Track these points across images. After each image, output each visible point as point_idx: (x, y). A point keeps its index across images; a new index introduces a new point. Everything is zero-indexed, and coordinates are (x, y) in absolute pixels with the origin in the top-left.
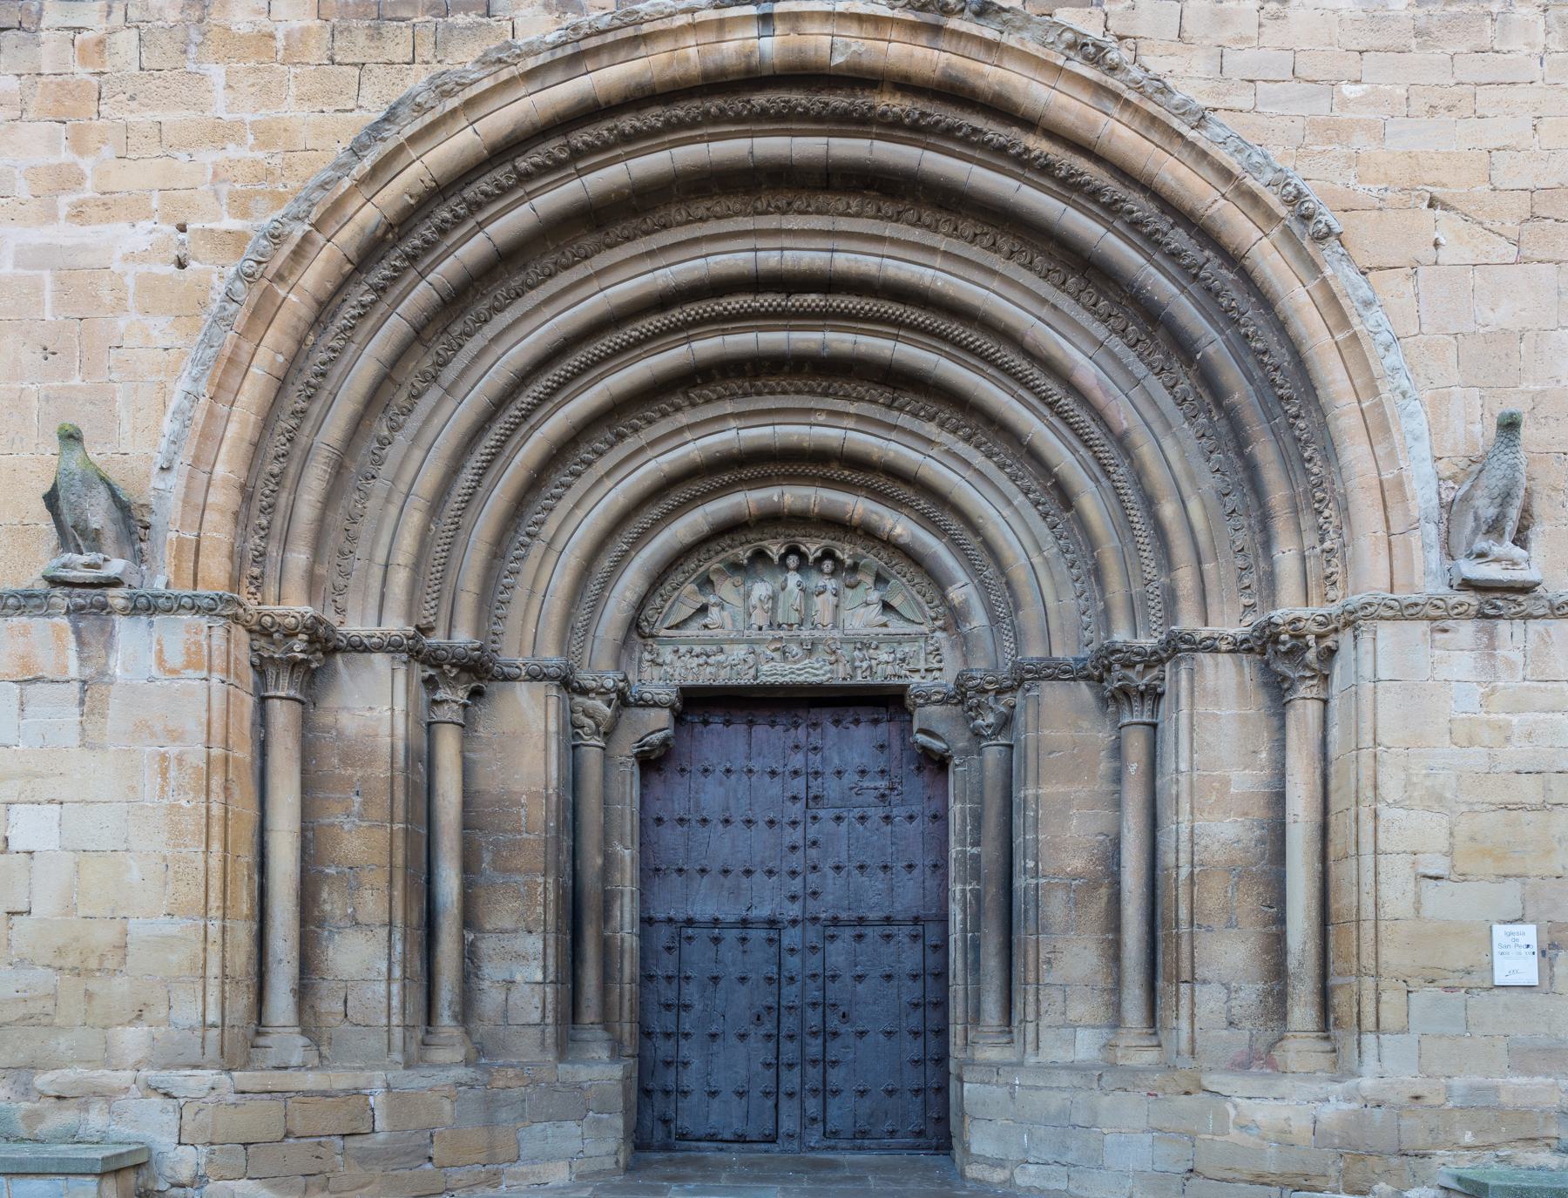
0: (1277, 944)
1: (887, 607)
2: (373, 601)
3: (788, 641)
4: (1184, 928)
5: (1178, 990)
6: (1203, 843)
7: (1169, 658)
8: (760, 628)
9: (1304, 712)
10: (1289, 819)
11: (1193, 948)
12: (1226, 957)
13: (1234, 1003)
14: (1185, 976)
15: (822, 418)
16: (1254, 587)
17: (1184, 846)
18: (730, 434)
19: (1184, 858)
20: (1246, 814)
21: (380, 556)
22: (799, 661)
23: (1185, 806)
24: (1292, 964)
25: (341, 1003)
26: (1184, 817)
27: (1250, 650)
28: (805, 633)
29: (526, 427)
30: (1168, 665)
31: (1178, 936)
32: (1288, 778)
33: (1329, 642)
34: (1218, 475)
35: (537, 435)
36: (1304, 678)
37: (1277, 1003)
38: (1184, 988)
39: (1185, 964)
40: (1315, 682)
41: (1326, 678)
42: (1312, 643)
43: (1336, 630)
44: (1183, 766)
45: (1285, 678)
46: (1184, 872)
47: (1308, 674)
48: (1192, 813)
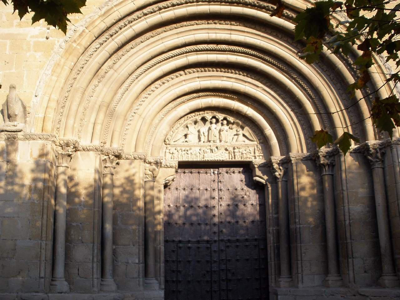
0: (376, 245)
1: (244, 135)
2: (90, 135)
3: (213, 146)
4: (349, 241)
5: (348, 260)
6: (352, 213)
7: (336, 154)
8: (204, 142)
9: (378, 172)
10: (377, 205)
11: (352, 247)
12: (361, 249)
13: (365, 264)
14: (350, 256)
15: (225, 79)
16: (359, 134)
17: (347, 214)
18: (198, 83)
19: (347, 217)
20: (363, 203)
21: (92, 120)
22: (217, 153)
23: (346, 201)
24: (383, 251)
25: (77, 270)
26: (346, 205)
27: (360, 152)
28: (218, 143)
29: (136, 81)
30: (336, 157)
31: (347, 243)
32: (375, 192)
33: (383, 151)
34: (345, 100)
35: (140, 83)
36: (377, 161)
37: (378, 265)
38: (350, 260)
39: (350, 253)
40: (380, 163)
41: (383, 162)
42: (378, 151)
43: (385, 147)
44: (345, 188)
45: (371, 161)
46: (347, 222)
47: (378, 160)
48: (348, 203)
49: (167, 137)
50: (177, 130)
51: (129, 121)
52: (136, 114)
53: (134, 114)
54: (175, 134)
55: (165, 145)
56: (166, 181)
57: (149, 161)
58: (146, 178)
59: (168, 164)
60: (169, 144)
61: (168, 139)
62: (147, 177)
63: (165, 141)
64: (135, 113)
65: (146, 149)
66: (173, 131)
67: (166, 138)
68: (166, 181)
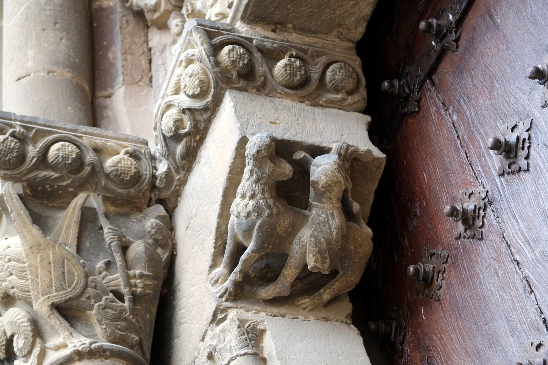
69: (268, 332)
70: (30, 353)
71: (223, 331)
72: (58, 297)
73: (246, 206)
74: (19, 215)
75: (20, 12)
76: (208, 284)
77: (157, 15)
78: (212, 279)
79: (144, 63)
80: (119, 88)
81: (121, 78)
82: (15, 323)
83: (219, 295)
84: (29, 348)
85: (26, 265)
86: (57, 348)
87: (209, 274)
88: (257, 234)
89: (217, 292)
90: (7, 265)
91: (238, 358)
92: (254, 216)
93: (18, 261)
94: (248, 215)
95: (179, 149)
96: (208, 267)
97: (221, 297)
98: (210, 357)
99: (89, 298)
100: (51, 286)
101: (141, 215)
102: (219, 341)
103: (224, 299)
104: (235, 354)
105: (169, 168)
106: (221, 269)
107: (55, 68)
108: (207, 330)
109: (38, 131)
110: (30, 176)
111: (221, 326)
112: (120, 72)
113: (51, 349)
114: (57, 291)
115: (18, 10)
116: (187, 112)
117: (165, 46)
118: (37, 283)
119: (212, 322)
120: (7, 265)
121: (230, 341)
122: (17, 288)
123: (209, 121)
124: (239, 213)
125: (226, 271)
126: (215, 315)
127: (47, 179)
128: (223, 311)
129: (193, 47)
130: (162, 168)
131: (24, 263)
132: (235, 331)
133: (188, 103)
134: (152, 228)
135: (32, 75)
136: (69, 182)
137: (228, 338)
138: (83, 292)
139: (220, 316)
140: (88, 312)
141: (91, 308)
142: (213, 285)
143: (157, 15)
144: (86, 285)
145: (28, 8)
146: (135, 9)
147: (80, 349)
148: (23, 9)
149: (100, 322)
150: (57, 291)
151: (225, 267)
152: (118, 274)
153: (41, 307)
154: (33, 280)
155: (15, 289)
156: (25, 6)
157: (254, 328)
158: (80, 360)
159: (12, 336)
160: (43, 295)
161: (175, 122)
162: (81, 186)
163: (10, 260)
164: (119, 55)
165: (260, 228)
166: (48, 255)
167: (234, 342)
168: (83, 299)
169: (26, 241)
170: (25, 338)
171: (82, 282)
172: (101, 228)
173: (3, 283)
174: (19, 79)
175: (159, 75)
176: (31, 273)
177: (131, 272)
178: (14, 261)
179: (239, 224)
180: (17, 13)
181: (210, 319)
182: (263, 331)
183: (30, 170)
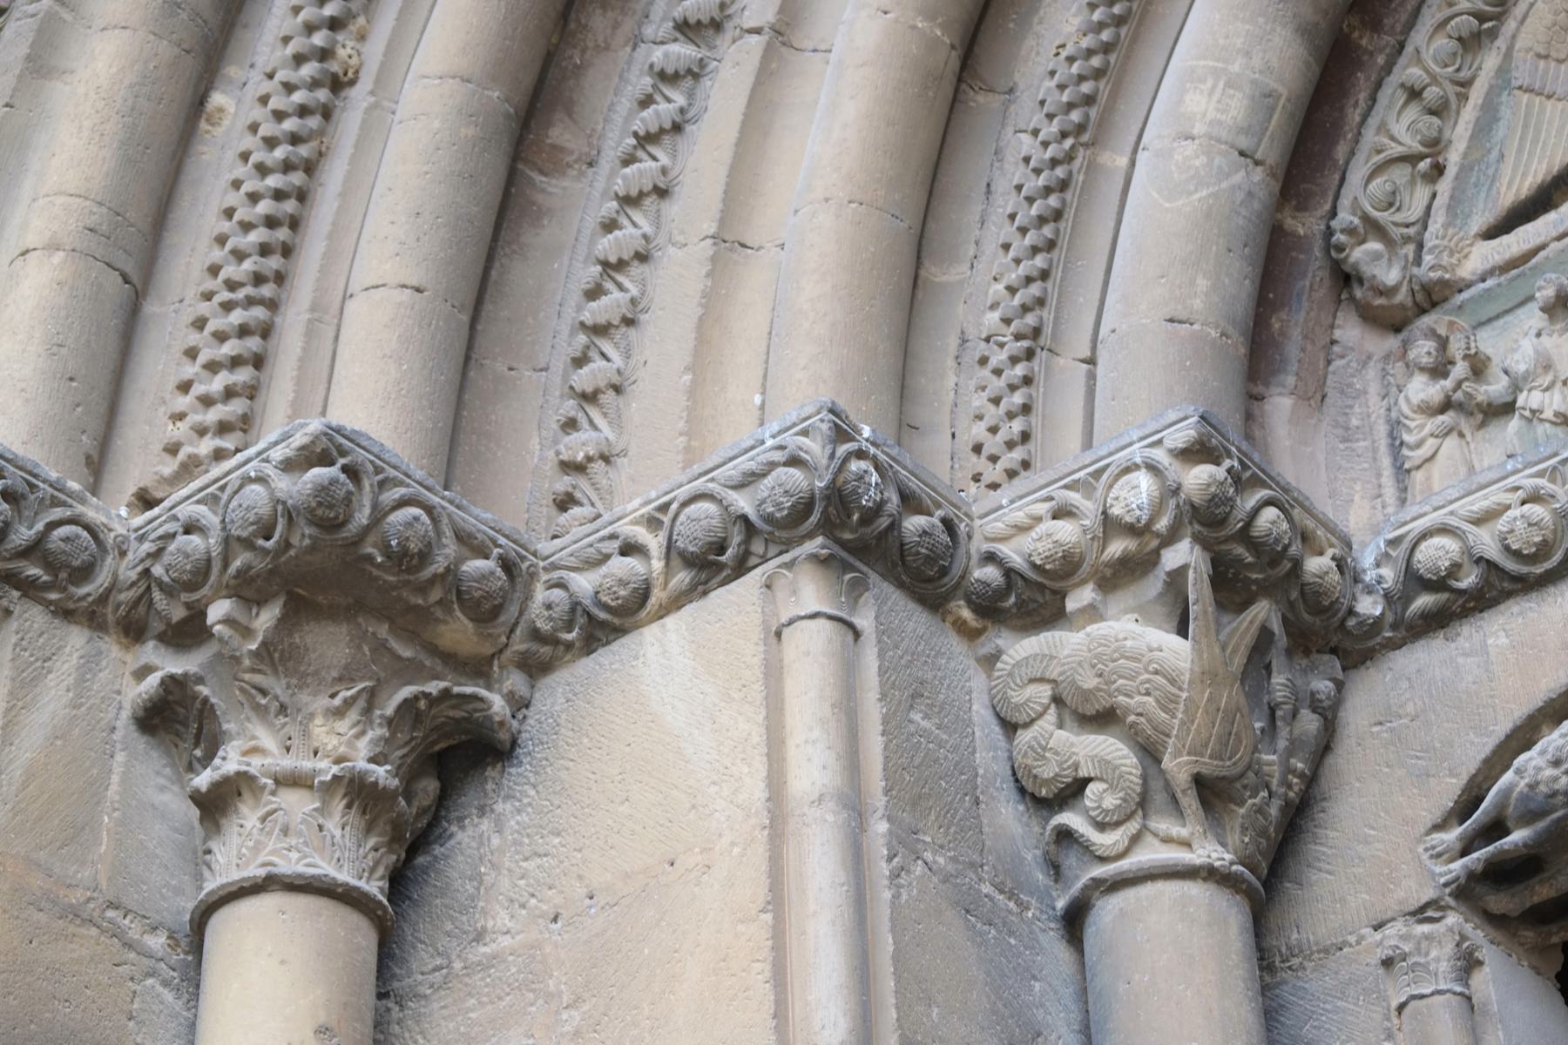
49: (1345, 202)
50: (1490, 61)
51: (628, 160)
52: (722, 42)
53: (682, 52)
54: (1469, 114)
55: (1392, 342)
56: (1496, 828)
57: (1017, 561)
58: (1070, 860)
59: (1436, 553)
60: (1432, 296)
61: (1374, 228)
62: (1065, 836)
63: (1345, 278)
64: (687, 29)
65: (979, 431)
66: (1414, 94)
67: (1345, 217)
68: (1496, 828)
69: (1486, 969)
70: (1118, 824)
71: (1428, 937)
72: (1209, 766)
73: (1556, 779)
74: (1205, 612)
75: (1197, 196)
76: (1420, 849)
77: (1379, 301)
78: (1433, 847)
79: (1322, 364)
80: (1280, 394)
81: (1291, 380)
82: (1116, 768)
83: (1442, 880)
84: (1123, 817)
85: (1184, 695)
86: (1167, 840)
87: (1428, 833)
88: (1549, 827)
89: (1441, 875)
90: (1146, 676)
91: (1448, 996)
92: (1560, 799)
93: (1172, 682)
94: (1554, 794)
95: (1424, 601)
96: (1429, 825)
97: (1446, 885)
98: (1387, 963)
99: (1245, 787)
100: (1206, 746)
101: (1304, 662)
102: (1418, 950)
103: (1448, 890)
104: (1442, 987)
105: (1382, 614)
106: (1453, 835)
107: (1230, 330)
108: (1393, 919)
109: (1254, 475)
110: (1224, 547)
111: (1426, 928)
112: (1294, 367)
113: (1156, 835)
114: (1211, 757)
115: (1196, 190)
116: (1483, 565)
117: (1369, 357)
118: (1189, 730)
119: (1413, 914)
120: (1146, 676)
121: (1437, 960)
122: (1149, 721)
123: (1509, 595)
124: (1538, 783)
125: (1458, 846)
126: (1423, 909)
127: (1239, 560)
128: (1442, 908)
129: (1553, 480)
130: (1369, 606)
131: (1180, 689)
132: (1449, 948)
133: (1492, 551)
134: (1328, 698)
135: (1196, 327)
136: (1260, 576)
137: (1434, 954)
138: (1242, 775)
139: (1430, 913)
140: (1233, 807)
141: (1241, 803)
142: (1432, 857)
143: (1379, 301)
144: (1249, 767)
145: (1214, 195)
146: (1347, 268)
147: (1217, 864)
148: (1204, 193)
149: (1244, 830)
150: (1211, 757)
151: (1460, 838)
152: (1274, 757)
153: (1178, 766)
154: (1183, 723)
155: (1142, 719)
156: (1211, 190)
157: (1471, 954)
158: (1205, 879)
159: (1088, 780)
160: (1189, 754)
161: (1452, 565)
162: (1266, 589)
163: (1156, 672)
164: (1296, 334)
165: (1559, 820)
166: (1221, 696)
167: (1444, 966)
168: (1238, 785)
169: (1201, 658)
170: (1124, 800)
171: (1247, 759)
172: (1268, 668)
173: (1121, 698)
174: (1171, 320)
175: (1351, 407)
176: (1185, 712)
177: (1293, 761)
178: (1165, 677)
179: (1524, 798)
180: (1190, 194)
181: (1412, 908)
182: (1480, 963)
183: (1227, 540)
